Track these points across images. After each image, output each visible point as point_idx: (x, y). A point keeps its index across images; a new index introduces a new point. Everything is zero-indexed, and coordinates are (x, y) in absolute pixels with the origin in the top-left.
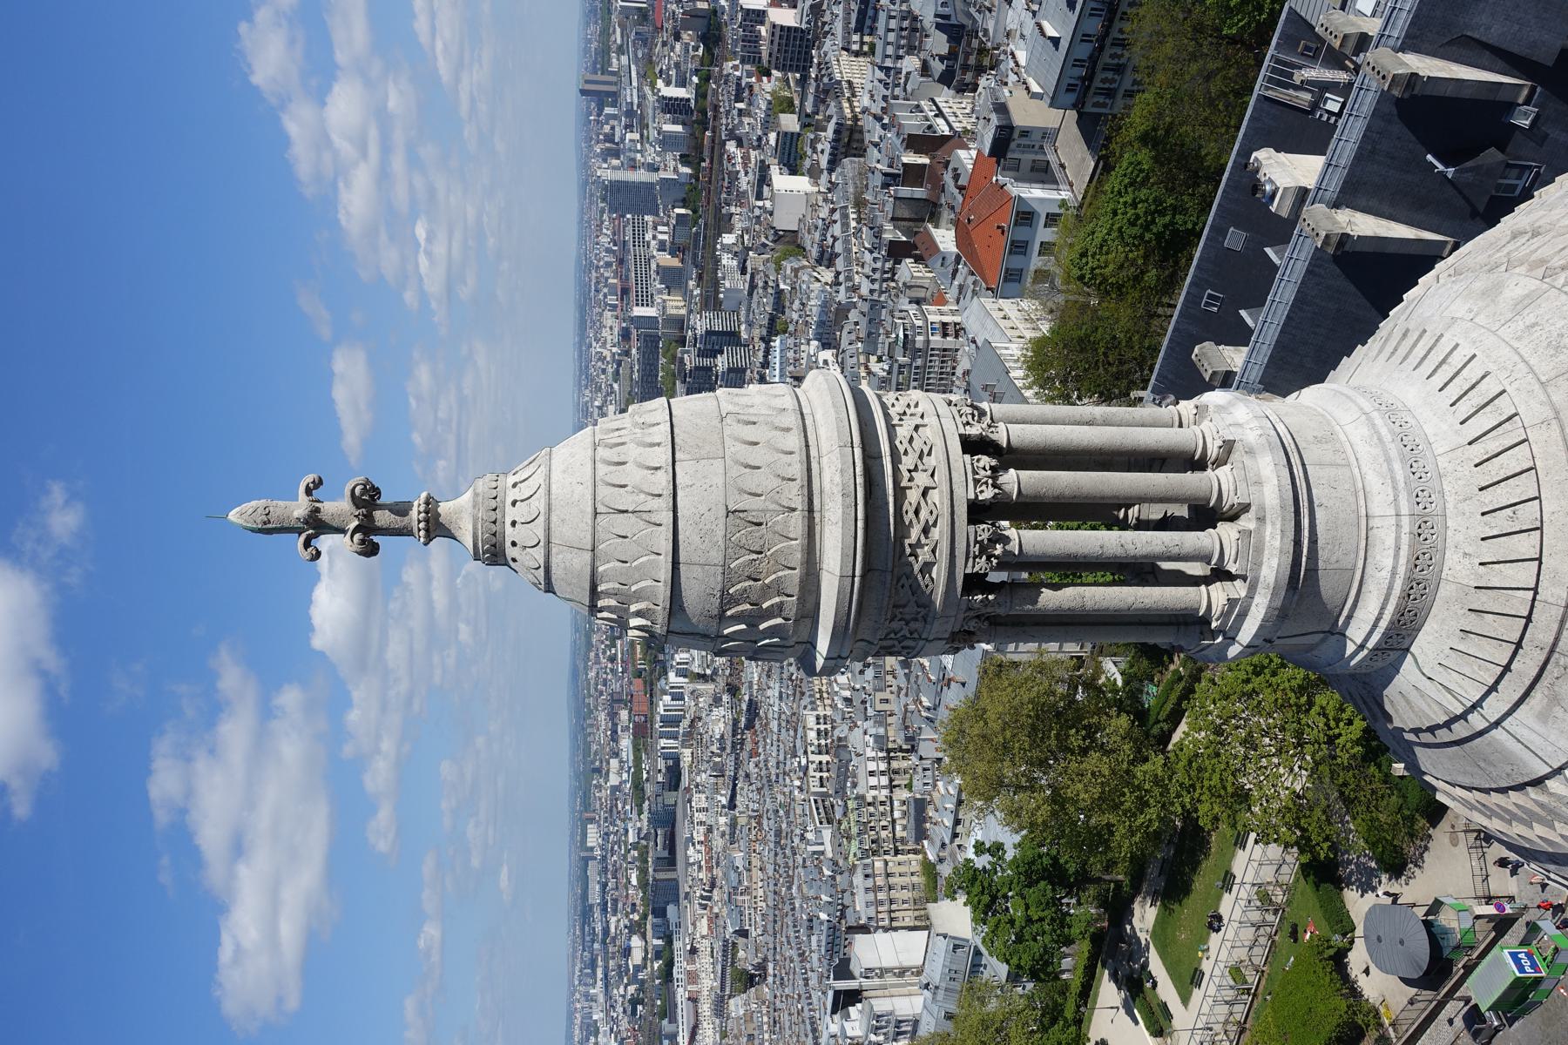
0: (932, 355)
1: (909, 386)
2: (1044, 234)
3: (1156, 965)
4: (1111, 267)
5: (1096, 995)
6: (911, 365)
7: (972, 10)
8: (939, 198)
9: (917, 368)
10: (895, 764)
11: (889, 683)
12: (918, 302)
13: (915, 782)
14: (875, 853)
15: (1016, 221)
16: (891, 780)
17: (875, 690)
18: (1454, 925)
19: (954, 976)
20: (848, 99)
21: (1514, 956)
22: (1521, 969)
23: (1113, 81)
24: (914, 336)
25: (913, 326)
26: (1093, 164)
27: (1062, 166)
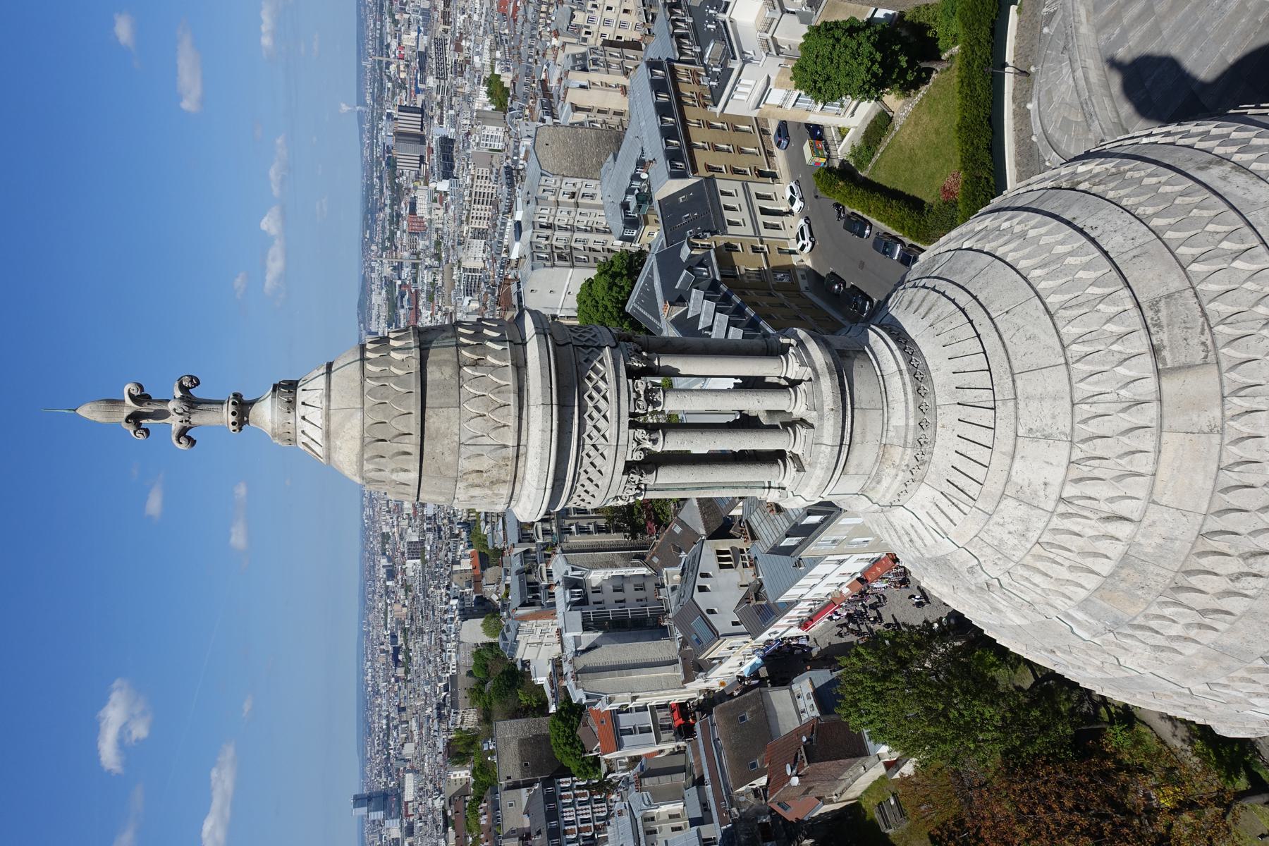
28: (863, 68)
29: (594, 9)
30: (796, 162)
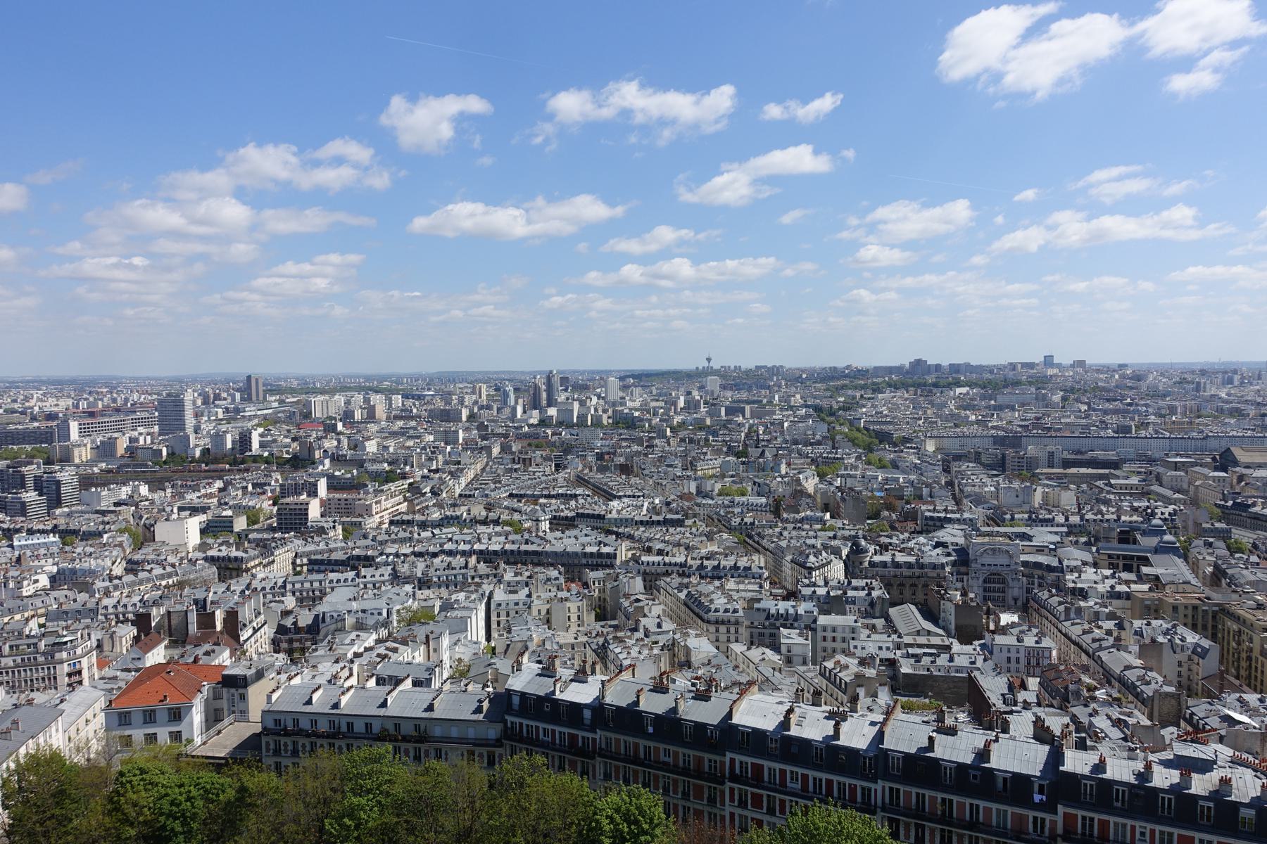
0: (49, 668)
1: (16, 655)
2: (163, 734)
4: (134, 797)
6: (38, 653)
7: (329, 637)
8: (190, 644)
9: (35, 659)
12: (99, 646)
15: (172, 709)
20: (261, 563)
23: (286, 752)
24: (66, 650)
25: (75, 647)
26: (222, 755)
27: (219, 732)
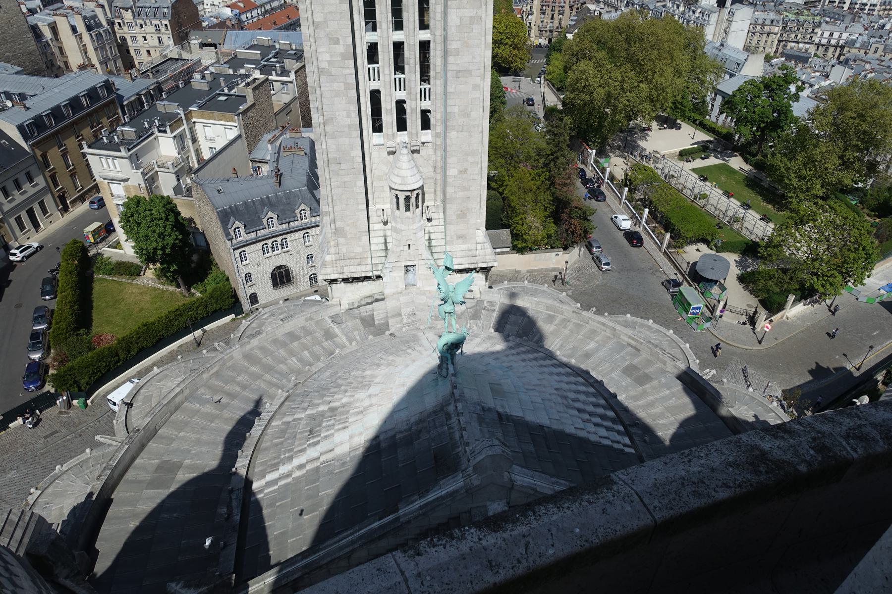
3: (713, 161)
5: (700, 130)
10: (831, 49)
11: (887, 55)
13: (819, 60)
14: (784, 28)
16: (823, 45)
17: (886, 46)
18: (712, 291)
19: (723, 61)
21: (699, 308)
22: (694, 308)
28: (154, 244)
29: (139, 26)
30: (84, 220)
